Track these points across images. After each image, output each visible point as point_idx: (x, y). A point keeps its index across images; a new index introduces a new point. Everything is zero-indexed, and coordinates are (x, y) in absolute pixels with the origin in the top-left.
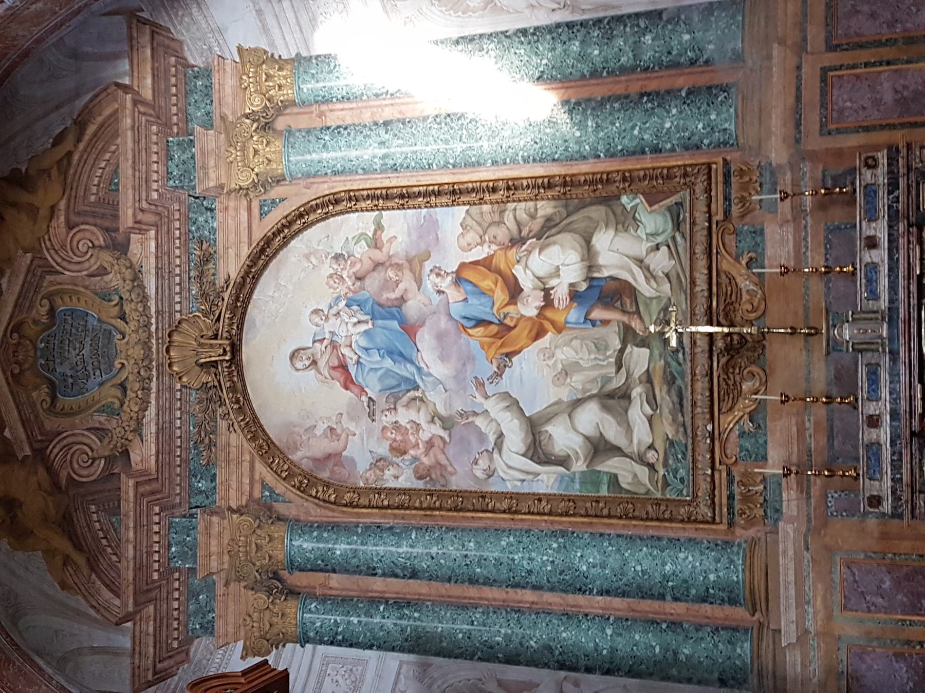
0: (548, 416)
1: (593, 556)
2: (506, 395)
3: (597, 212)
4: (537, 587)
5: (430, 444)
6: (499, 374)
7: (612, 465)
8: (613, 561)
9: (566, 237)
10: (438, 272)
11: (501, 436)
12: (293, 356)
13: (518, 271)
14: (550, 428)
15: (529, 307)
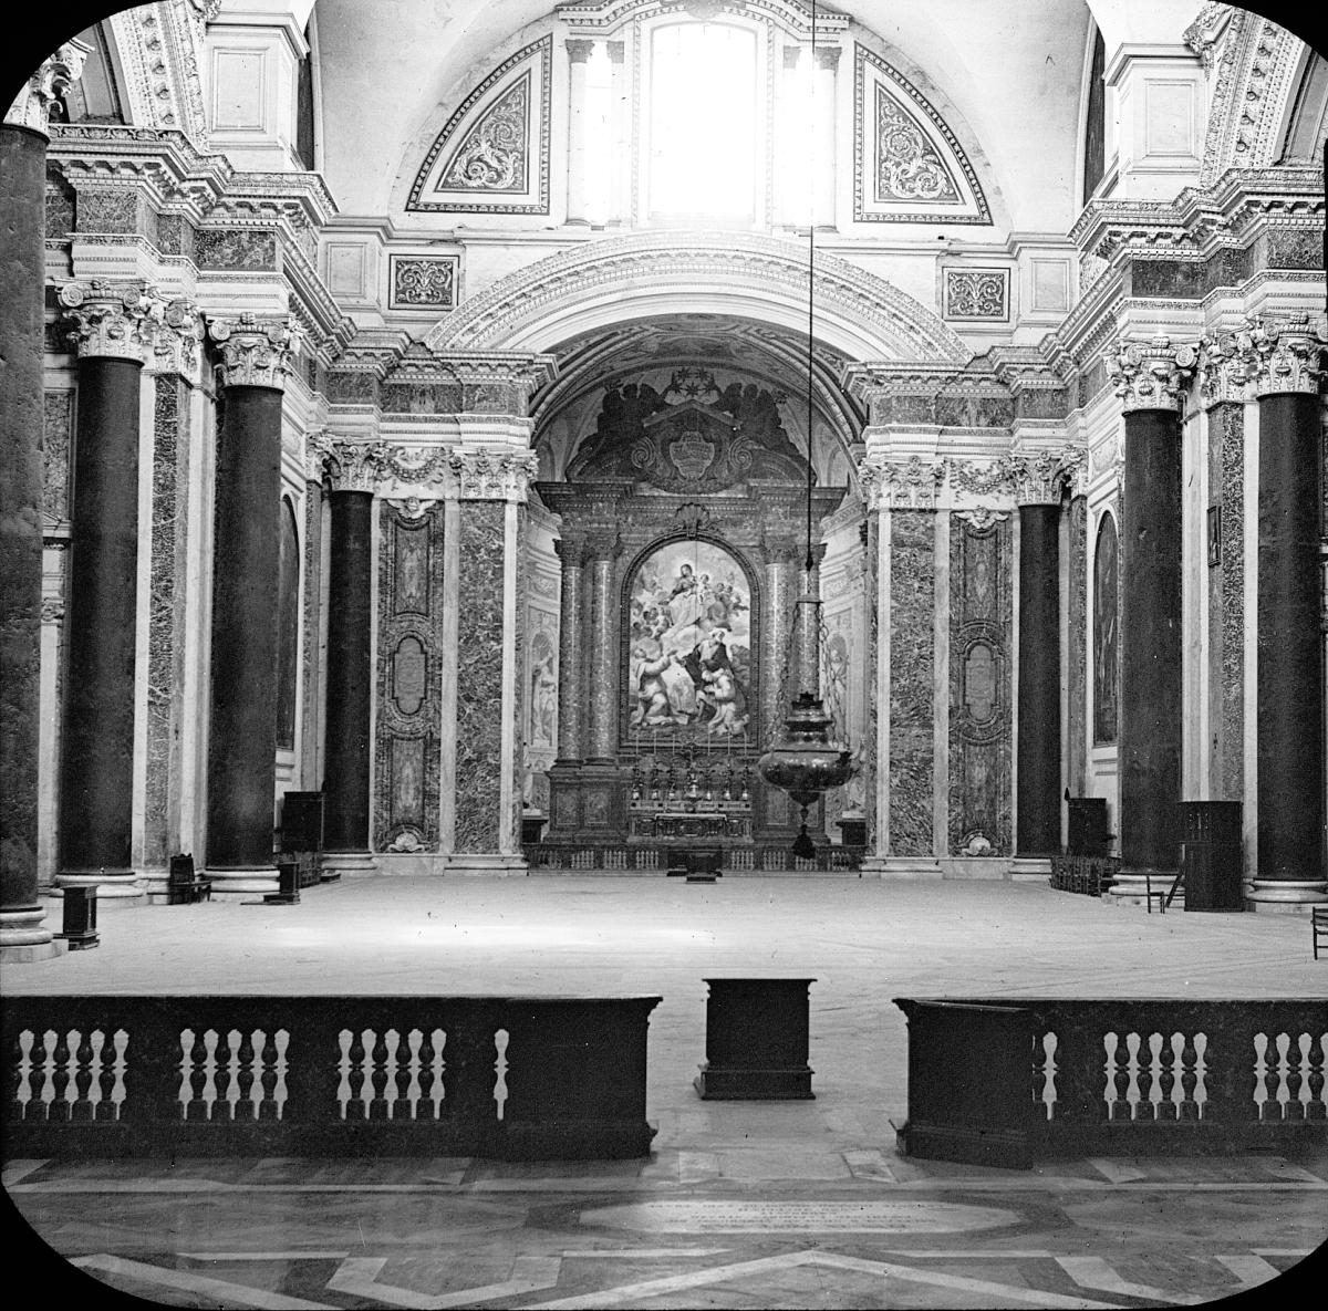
0: (661, 682)
1: (604, 700)
2: (669, 664)
3: (743, 705)
4: (591, 675)
5: (649, 630)
6: (679, 662)
7: (641, 709)
8: (602, 708)
9: (733, 692)
10: (722, 635)
11: (652, 661)
12: (688, 566)
13: (721, 670)
14: (655, 684)
15: (706, 675)
